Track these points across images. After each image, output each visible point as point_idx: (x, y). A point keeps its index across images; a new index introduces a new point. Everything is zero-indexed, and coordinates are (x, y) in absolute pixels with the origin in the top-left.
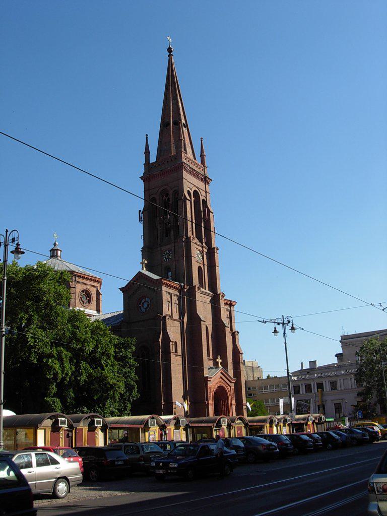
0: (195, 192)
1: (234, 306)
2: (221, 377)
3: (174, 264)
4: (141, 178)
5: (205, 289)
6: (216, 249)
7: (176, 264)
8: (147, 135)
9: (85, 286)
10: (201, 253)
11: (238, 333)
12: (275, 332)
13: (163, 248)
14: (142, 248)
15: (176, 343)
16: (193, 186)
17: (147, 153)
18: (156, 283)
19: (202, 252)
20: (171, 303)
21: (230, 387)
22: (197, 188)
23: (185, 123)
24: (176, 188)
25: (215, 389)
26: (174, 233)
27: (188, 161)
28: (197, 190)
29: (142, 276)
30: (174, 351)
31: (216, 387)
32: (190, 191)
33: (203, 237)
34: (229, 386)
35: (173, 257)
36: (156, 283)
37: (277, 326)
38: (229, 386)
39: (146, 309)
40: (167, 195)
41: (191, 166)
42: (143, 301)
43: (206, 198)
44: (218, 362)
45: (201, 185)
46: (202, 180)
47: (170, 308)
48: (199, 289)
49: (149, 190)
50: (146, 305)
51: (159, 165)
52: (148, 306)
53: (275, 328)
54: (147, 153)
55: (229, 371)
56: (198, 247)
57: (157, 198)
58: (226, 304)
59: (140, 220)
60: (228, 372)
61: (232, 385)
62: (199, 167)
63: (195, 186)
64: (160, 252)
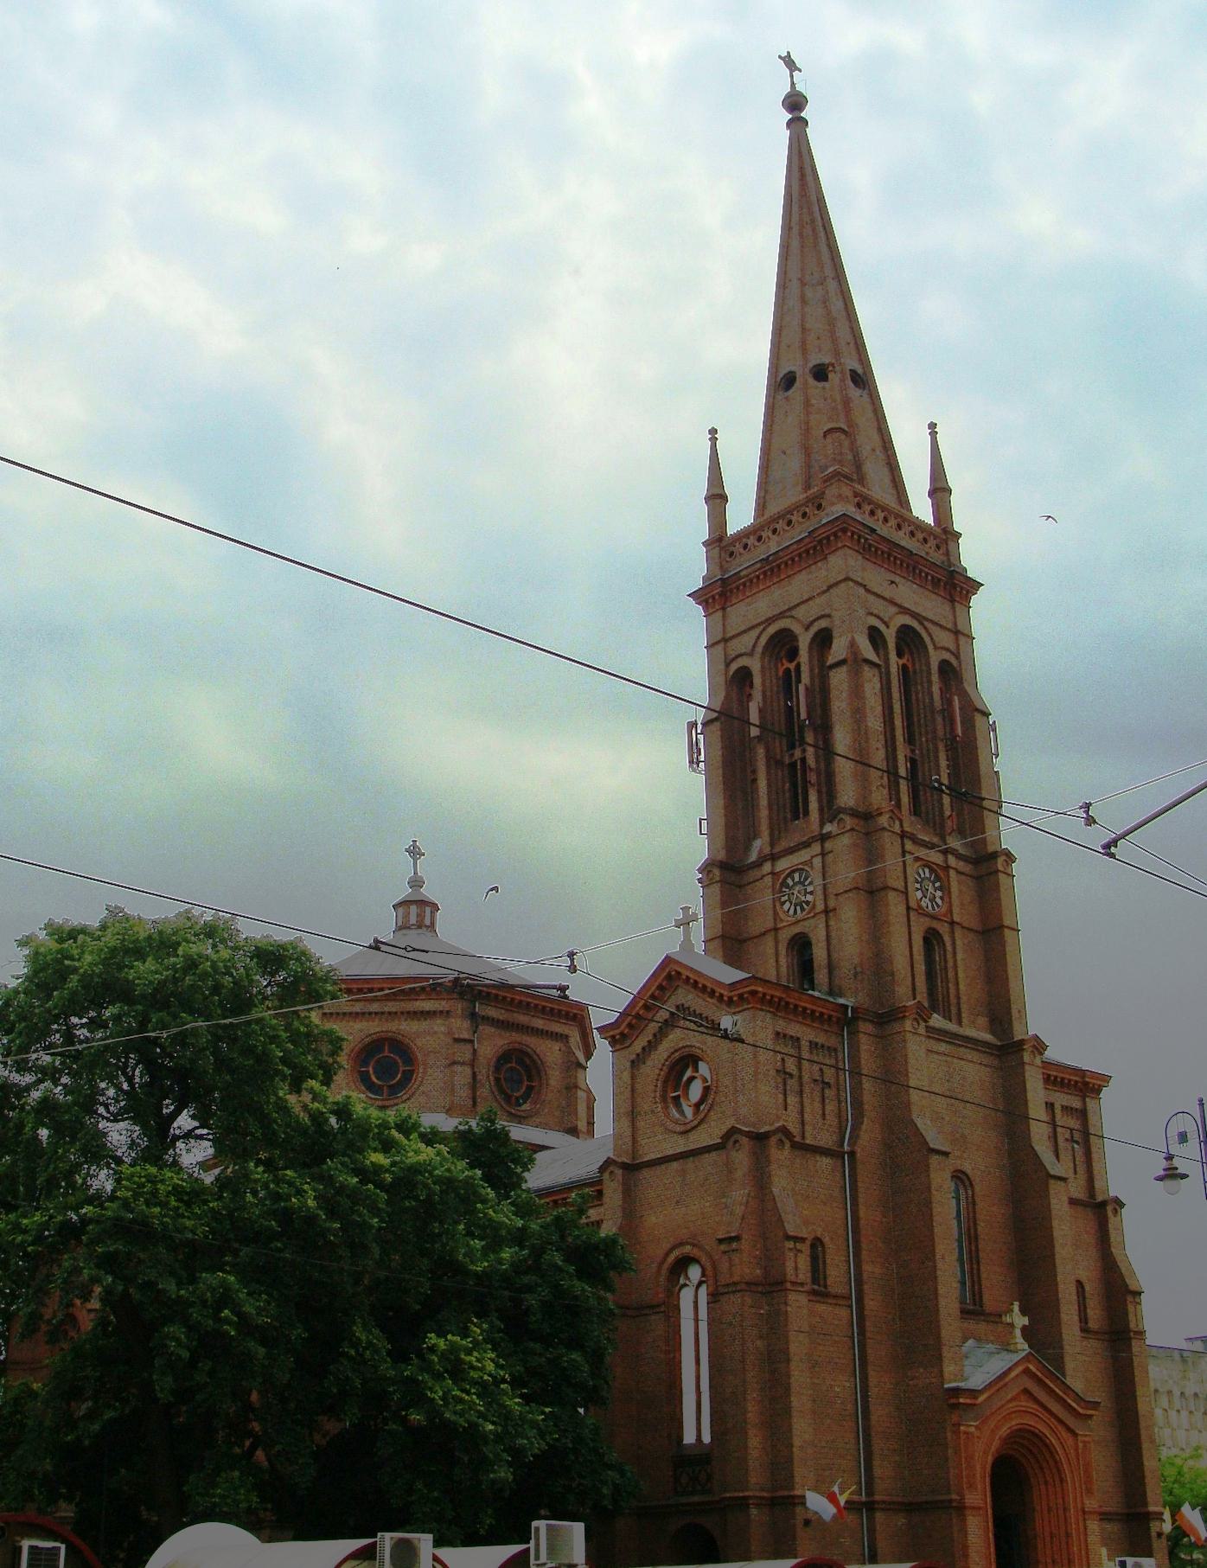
0: (905, 633)
1: (1098, 1090)
2: (1026, 1391)
3: (822, 926)
5: (960, 1023)
6: (1000, 860)
7: (832, 923)
8: (713, 431)
9: (516, 1037)
10: (938, 878)
11: (1122, 1205)
12: (1171, 1174)
13: (783, 864)
14: (700, 870)
15: (817, 1243)
16: (894, 609)
17: (717, 498)
18: (730, 999)
19: (940, 874)
20: (800, 1077)
21: (1075, 1435)
22: (915, 615)
23: (860, 371)
24: (823, 624)
25: (996, 1444)
26: (820, 801)
27: (872, 513)
28: (915, 624)
29: (679, 973)
30: (804, 1275)
31: (1004, 1431)
32: (882, 628)
33: (948, 813)
34: (1069, 1430)
36: (730, 999)
37: (1175, 1149)
38: (1069, 1430)
39: (697, 1106)
40: (793, 654)
41: (883, 530)
42: (689, 1073)
43: (957, 656)
44: (1012, 1325)
45: (930, 605)
46: (936, 582)
47: (792, 1100)
48: (922, 1015)
49: (725, 640)
50: (696, 1091)
51: (760, 539)
52: (706, 1090)
53: (1170, 1158)
54: (717, 498)
55: (1070, 1365)
56: (922, 852)
57: (755, 665)
58: (1055, 1082)
59: (691, 762)
60: (1061, 1367)
61: (1096, 1434)
62: (920, 536)
63: (905, 611)
64: (768, 880)
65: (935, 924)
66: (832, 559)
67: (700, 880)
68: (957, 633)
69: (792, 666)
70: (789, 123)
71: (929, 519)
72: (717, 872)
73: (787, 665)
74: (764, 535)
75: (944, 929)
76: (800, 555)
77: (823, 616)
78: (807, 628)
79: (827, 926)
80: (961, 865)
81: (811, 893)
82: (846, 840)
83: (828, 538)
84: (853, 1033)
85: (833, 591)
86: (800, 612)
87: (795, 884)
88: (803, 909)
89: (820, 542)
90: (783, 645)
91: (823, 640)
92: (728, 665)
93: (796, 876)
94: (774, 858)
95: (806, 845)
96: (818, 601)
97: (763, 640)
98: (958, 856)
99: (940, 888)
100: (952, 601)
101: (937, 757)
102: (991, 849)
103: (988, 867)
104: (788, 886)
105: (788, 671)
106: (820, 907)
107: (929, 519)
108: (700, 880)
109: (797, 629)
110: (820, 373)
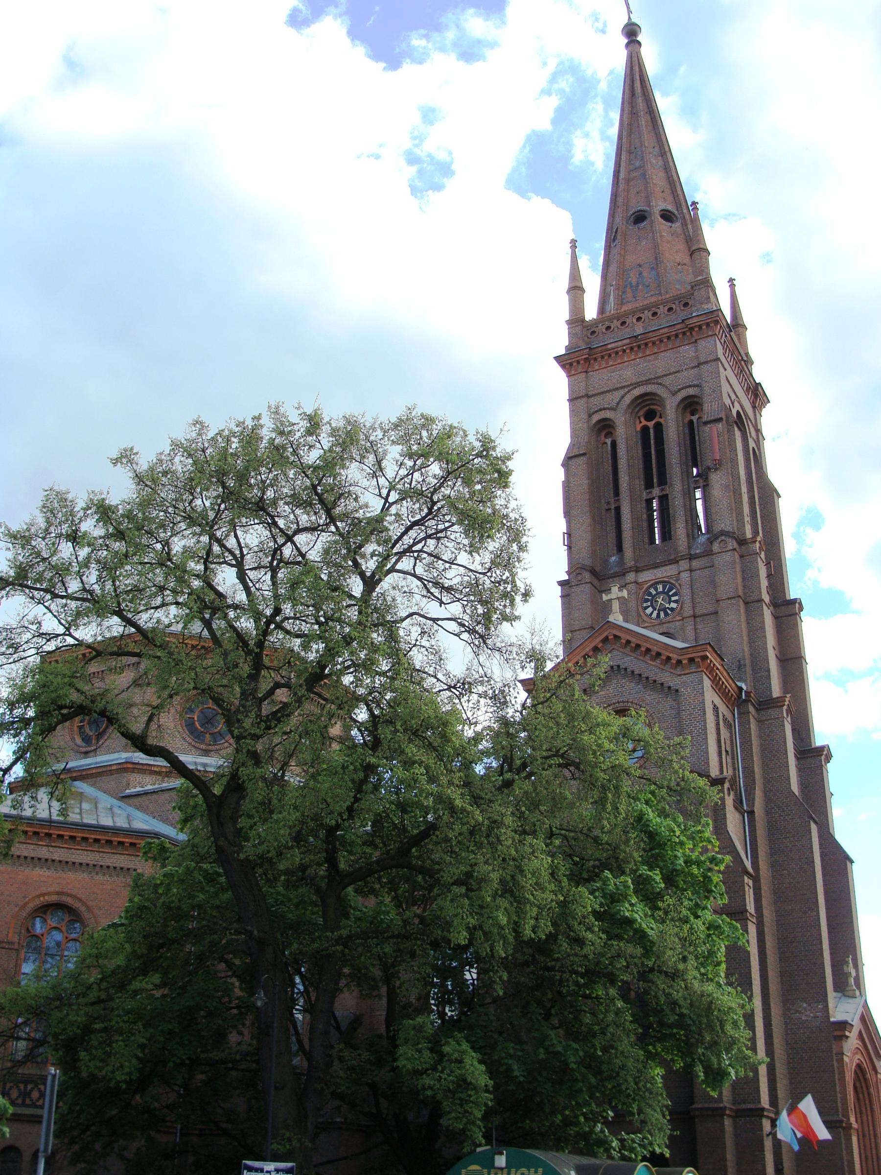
4: (558, 359)
13: (646, 576)
17: (576, 289)
18: (679, 662)
24: (691, 391)
29: (616, 637)
35: (688, 605)
36: (679, 662)
54: (576, 289)
66: (702, 344)
67: (562, 583)
69: (651, 424)
70: (627, 46)
72: (587, 576)
73: (644, 423)
74: (628, 321)
76: (669, 338)
77: (695, 386)
78: (674, 394)
79: (696, 629)
81: (675, 601)
82: (727, 557)
83: (700, 327)
84: (744, 714)
85: (705, 368)
86: (667, 381)
87: (658, 593)
88: (666, 614)
89: (691, 329)
90: (647, 406)
91: (691, 405)
92: (590, 416)
93: (660, 588)
94: (637, 570)
95: (676, 561)
96: (685, 373)
97: (628, 399)
103: (787, 612)
104: (650, 594)
105: (645, 429)
106: (688, 612)
108: (562, 583)
109: (661, 392)
110: (667, 216)
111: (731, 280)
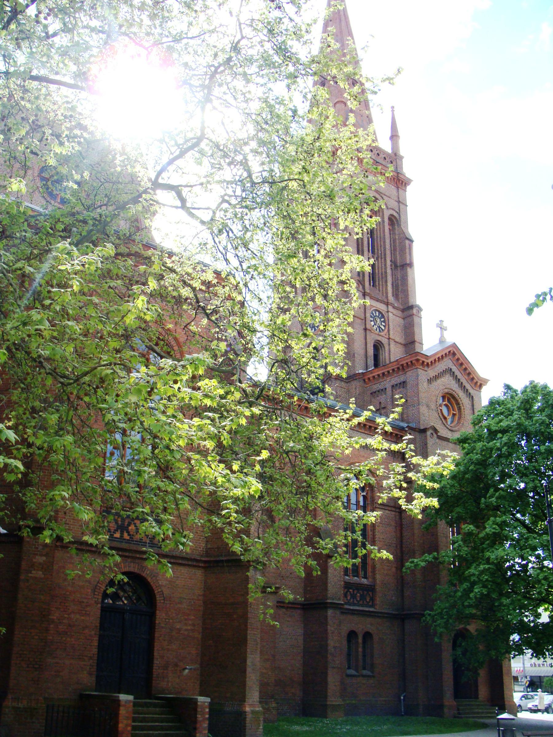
6: (415, 311)
43: (399, 214)
65: (379, 338)
68: (399, 202)
71: (390, 151)
75: (385, 341)
80: (395, 311)
98: (394, 307)
99: (384, 322)
100: (398, 188)
101: (385, 260)
102: (410, 304)
107: (390, 151)
111: (393, 107)
